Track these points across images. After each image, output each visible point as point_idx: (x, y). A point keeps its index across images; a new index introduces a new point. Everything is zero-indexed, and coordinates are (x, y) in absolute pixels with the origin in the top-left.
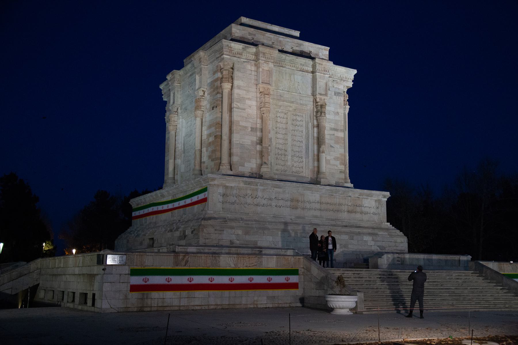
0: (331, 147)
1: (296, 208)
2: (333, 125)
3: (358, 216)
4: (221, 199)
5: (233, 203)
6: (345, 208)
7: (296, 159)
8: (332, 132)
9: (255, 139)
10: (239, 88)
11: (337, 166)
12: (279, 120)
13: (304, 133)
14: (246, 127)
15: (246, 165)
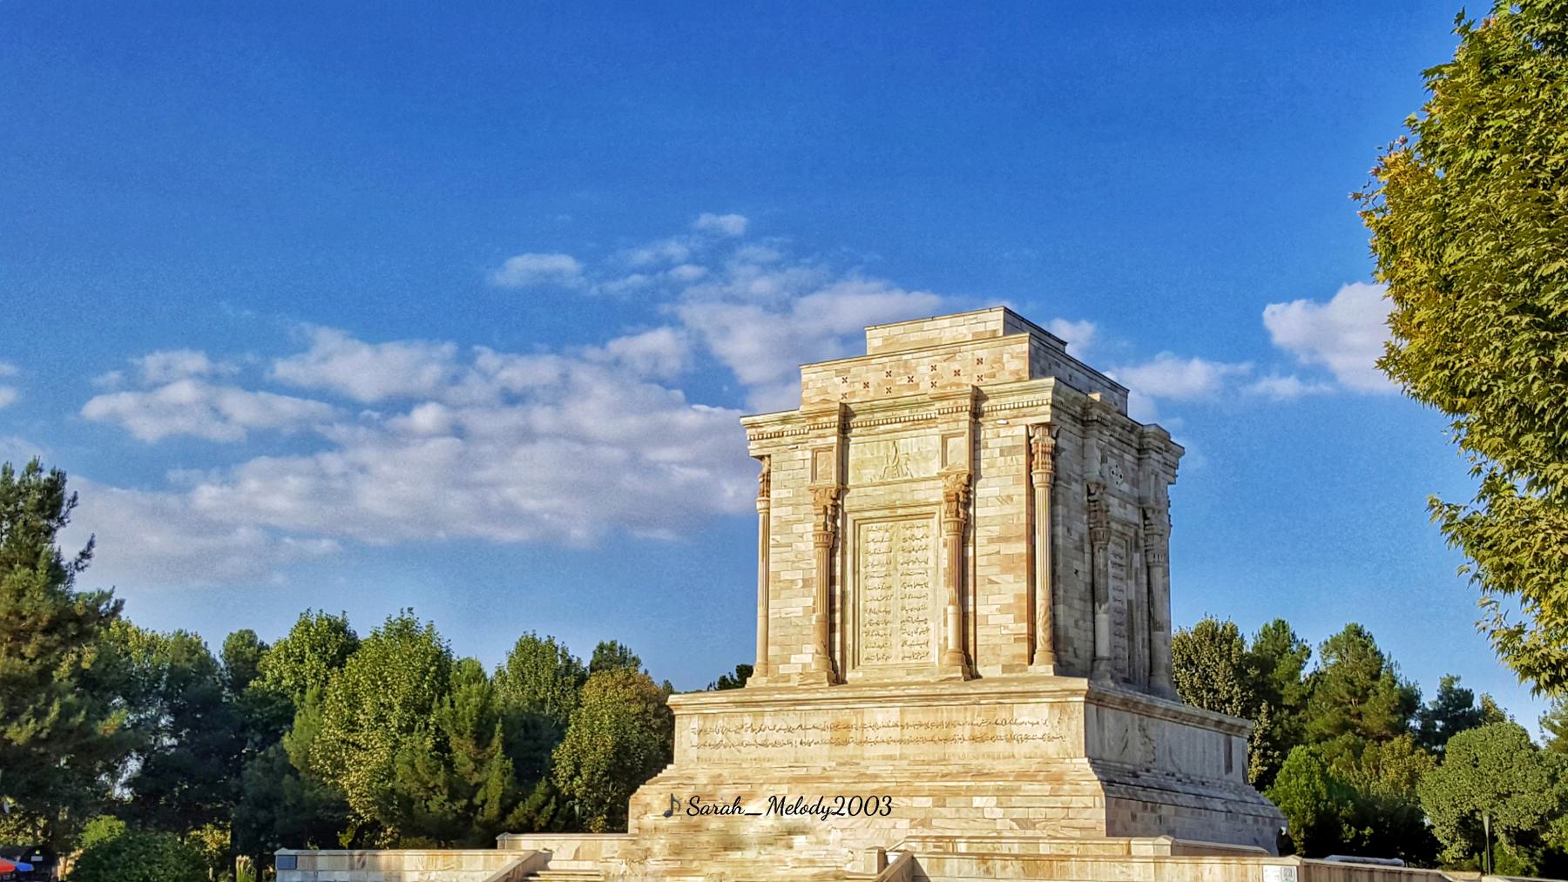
0: (991, 582)
1: (846, 743)
2: (996, 531)
3: (1000, 747)
4: (695, 739)
5: (717, 746)
6: (967, 732)
7: (911, 627)
8: (994, 547)
9: (810, 602)
10: (780, 504)
11: (1006, 628)
12: (872, 547)
13: (931, 563)
14: (792, 581)
15: (793, 659)
